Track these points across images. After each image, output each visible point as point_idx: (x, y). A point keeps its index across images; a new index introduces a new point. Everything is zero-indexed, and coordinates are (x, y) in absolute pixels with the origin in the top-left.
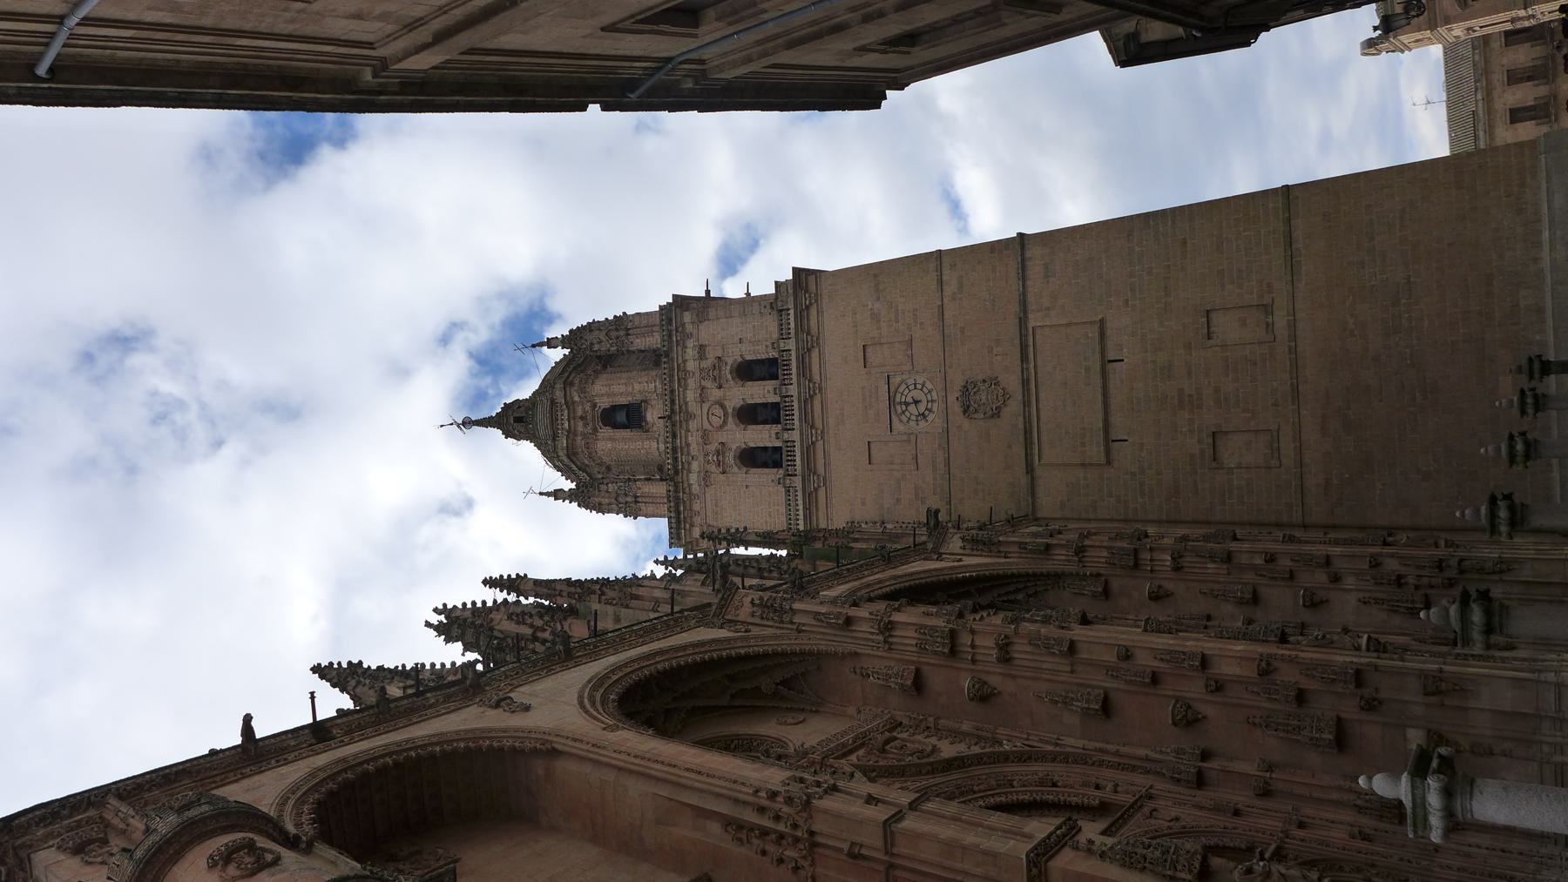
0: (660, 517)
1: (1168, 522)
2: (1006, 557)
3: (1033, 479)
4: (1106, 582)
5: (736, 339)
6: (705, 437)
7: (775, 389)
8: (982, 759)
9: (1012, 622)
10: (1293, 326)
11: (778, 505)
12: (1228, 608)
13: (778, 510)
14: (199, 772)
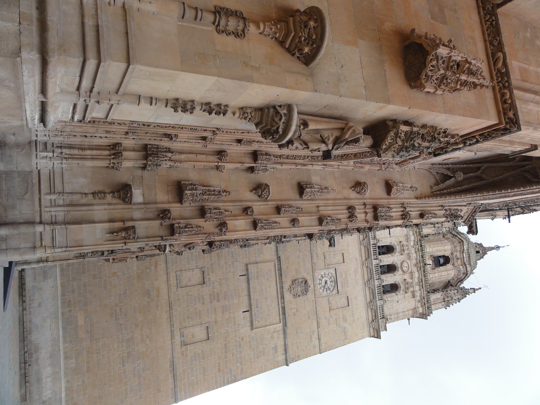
3: (277, 254)
5: (400, 302)
6: (409, 258)
7: (383, 282)
8: (370, 154)
10: (172, 337)
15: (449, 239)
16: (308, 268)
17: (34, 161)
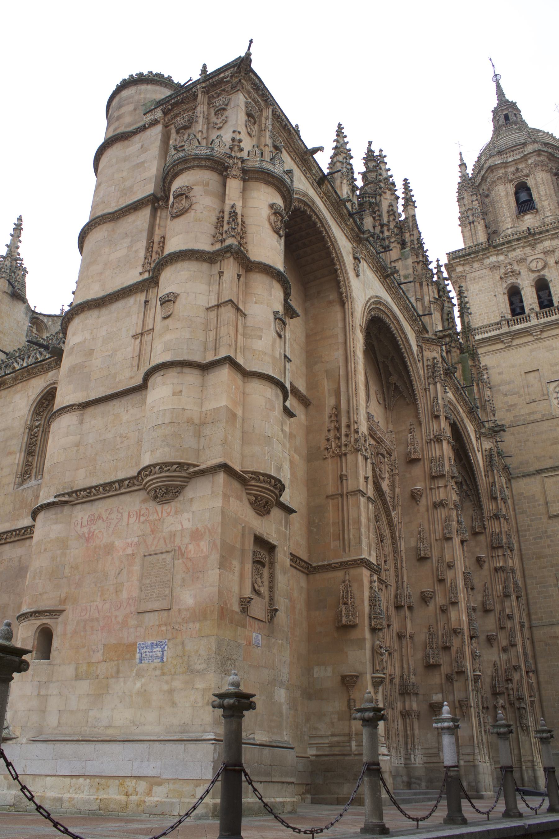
0: (464, 242)
1: (521, 555)
2: (485, 475)
3: (533, 474)
4: (482, 533)
6: (521, 261)
9: (455, 506)
11: (488, 318)
12: (480, 598)
13: (485, 319)
14: (292, 138)
15: (489, 188)
16: (550, 426)
17: (417, 765)
